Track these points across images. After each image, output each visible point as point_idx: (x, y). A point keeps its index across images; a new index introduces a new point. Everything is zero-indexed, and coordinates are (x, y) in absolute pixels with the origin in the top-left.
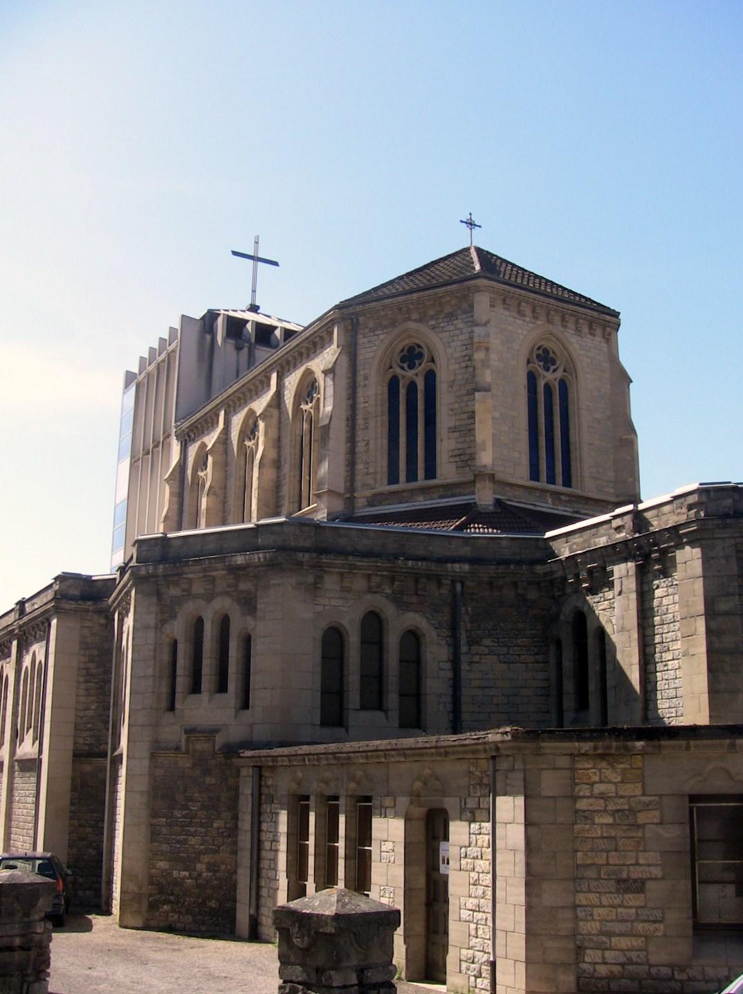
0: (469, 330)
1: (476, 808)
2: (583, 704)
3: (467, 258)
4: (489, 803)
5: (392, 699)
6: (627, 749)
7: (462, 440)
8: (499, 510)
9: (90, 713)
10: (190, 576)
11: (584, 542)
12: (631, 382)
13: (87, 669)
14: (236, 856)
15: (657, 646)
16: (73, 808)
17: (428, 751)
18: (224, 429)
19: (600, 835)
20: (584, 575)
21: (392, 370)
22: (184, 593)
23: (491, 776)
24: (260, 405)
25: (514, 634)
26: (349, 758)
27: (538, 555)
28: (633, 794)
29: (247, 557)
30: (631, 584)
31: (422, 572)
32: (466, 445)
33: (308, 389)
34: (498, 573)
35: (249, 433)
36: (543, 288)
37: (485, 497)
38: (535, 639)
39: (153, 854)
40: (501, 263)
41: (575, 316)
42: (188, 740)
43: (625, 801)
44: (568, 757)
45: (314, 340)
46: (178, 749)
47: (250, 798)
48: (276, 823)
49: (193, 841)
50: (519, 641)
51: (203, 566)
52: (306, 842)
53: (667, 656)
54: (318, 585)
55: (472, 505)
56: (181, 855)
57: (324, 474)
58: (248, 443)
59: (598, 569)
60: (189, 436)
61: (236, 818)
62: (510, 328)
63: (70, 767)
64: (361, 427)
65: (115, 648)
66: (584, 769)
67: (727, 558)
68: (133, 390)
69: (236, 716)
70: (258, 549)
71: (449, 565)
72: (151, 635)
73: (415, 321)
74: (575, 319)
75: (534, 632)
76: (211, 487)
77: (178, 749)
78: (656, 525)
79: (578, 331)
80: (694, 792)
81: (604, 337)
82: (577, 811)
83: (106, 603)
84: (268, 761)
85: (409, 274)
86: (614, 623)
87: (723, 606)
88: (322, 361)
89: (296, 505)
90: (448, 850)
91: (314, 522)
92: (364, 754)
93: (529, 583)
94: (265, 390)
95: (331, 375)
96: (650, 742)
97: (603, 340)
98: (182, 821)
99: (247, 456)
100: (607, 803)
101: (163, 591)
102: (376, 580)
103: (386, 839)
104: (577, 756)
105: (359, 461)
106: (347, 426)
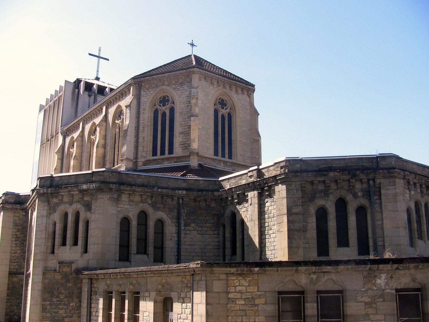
0: (190, 90)
1: (185, 297)
2: (234, 253)
3: (190, 59)
4: (190, 295)
5: (151, 249)
6: (251, 271)
7: (184, 137)
8: (200, 168)
9: (17, 255)
10: (63, 194)
11: (236, 182)
12: (259, 115)
13: (16, 235)
14: (80, 319)
15: (267, 227)
16: (8, 298)
17: (164, 271)
18: (82, 130)
19: (239, 309)
20: (235, 196)
21: (155, 106)
22: (59, 201)
23: (192, 283)
24: (97, 120)
25: (205, 222)
26: (130, 275)
27: (216, 187)
28: (253, 291)
29: (88, 186)
30: (256, 200)
31: (165, 194)
32: (187, 140)
33: (119, 114)
34: (198, 195)
35: (93, 133)
36: (222, 73)
37: (194, 163)
38: (214, 224)
39: (43, 318)
40: (205, 62)
41: (235, 86)
42: (60, 267)
43: (250, 294)
44: (225, 275)
45: (122, 92)
46: (55, 270)
47: (87, 293)
48: (98, 304)
49: (61, 312)
50: (207, 225)
51: (68, 189)
52: (111, 312)
53: (271, 232)
54: (119, 199)
55: (189, 166)
56: (56, 318)
57: (125, 151)
58: (92, 137)
59: (242, 194)
60: (67, 134)
61: (80, 301)
62: (207, 90)
63: (7, 279)
64: (141, 131)
65: (29, 225)
66: (232, 280)
67: (297, 190)
68: (42, 113)
69: (81, 256)
70: (93, 182)
71: (177, 191)
72: (45, 219)
73: (166, 85)
74: (236, 87)
75: (213, 221)
76: (75, 156)
77: (55, 270)
78: (267, 175)
79: (237, 92)
80: (280, 290)
81: (248, 95)
82: (229, 299)
83: (25, 205)
84: (95, 276)
85: (164, 65)
86: (248, 217)
87: (295, 210)
88: (125, 102)
89: (112, 165)
90: (173, 316)
91: (118, 171)
92: (137, 273)
93: (211, 200)
94: (100, 114)
95: (129, 108)
96: (262, 269)
97: (247, 96)
98: (56, 303)
99: (91, 143)
100: (242, 295)
101: (50, 200)
102: (144, 197)
103: (146, 311)
104: (229, 274)
105: (140, 146)
106: (135, 130)
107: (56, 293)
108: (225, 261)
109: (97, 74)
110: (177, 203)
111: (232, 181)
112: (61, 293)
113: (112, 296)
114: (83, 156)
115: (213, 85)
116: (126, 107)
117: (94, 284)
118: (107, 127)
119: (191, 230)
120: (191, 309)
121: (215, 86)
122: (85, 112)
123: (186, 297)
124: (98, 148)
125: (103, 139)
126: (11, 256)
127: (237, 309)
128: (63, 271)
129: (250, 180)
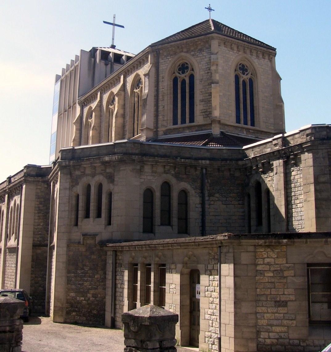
0: (209, 56)
1: (212, 269)
2: (260, 223)
3: (208, 24)
4: (218, 267)
5: (175, 221)
6: (279, 243)
7: (206, 105)
8: (222, 137)
9: (40, 227)
10: (85, 166)
11: (260, 151)
12: (281, 79)
13: (39, 207)
14: (105, 290)
15: (293, 197)
16: (33, 269)
17: (191, 244)
18: (100, 100)
19: (267, 281)
20: (260, 165)
21: (174, 74)
22: (82, 174)
23: (219, 255)
24: (116, 90)
25: (229, 192)
26: (155, 247)
27: (240, 156)
28: (282, 263)
29: (110, 157)
30: (281, 169)
31: (188, 164)
32: (208, 108)
33: (137, 82)
34: (222, 165)
35: (111, 102)
36: (242, 38)
37: (216, 131)
38: (238, 194)
39: (68, 290)
40: (223, 27)
41: (256, 50)
42: (84, 239)
43: (279, 266)
44: (253, 247)
45: (140, 61)
46: (79, 243)
47: (111, 265)
48: (123, 276)
49: (86, 284)
50: (231, 195)
51: (91, 161)
52: (137, 285)
53: (297, 201)
54: (142, 170)
55: (210, 134)
56: (81, 290)
57: (144, 120)
58: (110, 107)
59: (267, 163)
60: (84, 104)
61: (105, 273)
62: (227, 55)
63: (31, 251)
64: (161, 99)
65: (51, 198)
66: (260, 252)
67: (324, 158)
68: (59, 83)
69: (105, 228)
70: (114, 154)
71: (200, 161)
72: (67, 192)
73: (185, 52)
74: (256, 51)
75: (238, 191)
76: (94, 126)
77: (79, 243)
78: (292, 143)
79: (257, 57)
80: (309, 262)
81: (269, 60)
82: (257, 271)
83: (47, 178)
84: (119, 248)
85: (182, 31)
86: (273, 187)
87: (322, 179)
88: (143, 70)
89: (132, 134)
90: (199, 288)
91: (140, 142)
92: (162, 245)
93: (236, 169)
94: (118, 83)
95: (148, 77)
96: (290, 240)
97: (269, 61)
98: (81, 275)
99: (110, 112)
100: (270, 267)
101: (73, 172)
102: (167, 168)
103: (172, 283)
104: (257, 246)
105: (160, 115)
106: (155, 99)
107: (80, 265)
108: (250, 233)
109: (113, 42)
110: (200, 173)
111: (256, 149)
112: (85, 266)
113: (137, 268)
114: (102, 126)
115: (233, 50)
116: (145, 76)
117: (119, 256)
118: (126, 96)
119: (215, 200)
120: (219, 282)
121: (235, 52)
122: (102, 81)
123: (214, 269)
124: (117, 117)
125: (122, 108)
126: (34, 228)
127: (266, 281)
128: (87, 244)
129: (275, 148)
